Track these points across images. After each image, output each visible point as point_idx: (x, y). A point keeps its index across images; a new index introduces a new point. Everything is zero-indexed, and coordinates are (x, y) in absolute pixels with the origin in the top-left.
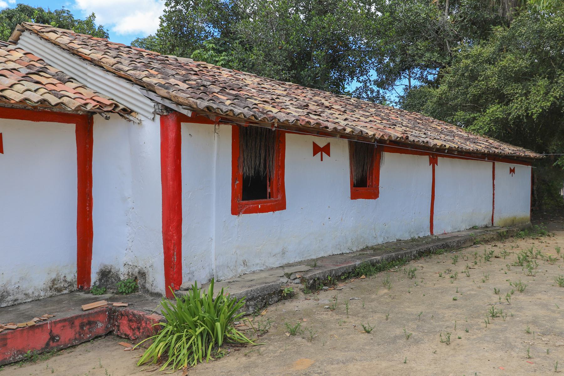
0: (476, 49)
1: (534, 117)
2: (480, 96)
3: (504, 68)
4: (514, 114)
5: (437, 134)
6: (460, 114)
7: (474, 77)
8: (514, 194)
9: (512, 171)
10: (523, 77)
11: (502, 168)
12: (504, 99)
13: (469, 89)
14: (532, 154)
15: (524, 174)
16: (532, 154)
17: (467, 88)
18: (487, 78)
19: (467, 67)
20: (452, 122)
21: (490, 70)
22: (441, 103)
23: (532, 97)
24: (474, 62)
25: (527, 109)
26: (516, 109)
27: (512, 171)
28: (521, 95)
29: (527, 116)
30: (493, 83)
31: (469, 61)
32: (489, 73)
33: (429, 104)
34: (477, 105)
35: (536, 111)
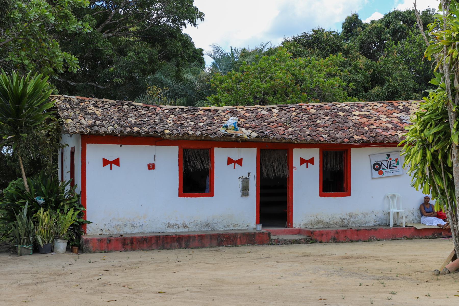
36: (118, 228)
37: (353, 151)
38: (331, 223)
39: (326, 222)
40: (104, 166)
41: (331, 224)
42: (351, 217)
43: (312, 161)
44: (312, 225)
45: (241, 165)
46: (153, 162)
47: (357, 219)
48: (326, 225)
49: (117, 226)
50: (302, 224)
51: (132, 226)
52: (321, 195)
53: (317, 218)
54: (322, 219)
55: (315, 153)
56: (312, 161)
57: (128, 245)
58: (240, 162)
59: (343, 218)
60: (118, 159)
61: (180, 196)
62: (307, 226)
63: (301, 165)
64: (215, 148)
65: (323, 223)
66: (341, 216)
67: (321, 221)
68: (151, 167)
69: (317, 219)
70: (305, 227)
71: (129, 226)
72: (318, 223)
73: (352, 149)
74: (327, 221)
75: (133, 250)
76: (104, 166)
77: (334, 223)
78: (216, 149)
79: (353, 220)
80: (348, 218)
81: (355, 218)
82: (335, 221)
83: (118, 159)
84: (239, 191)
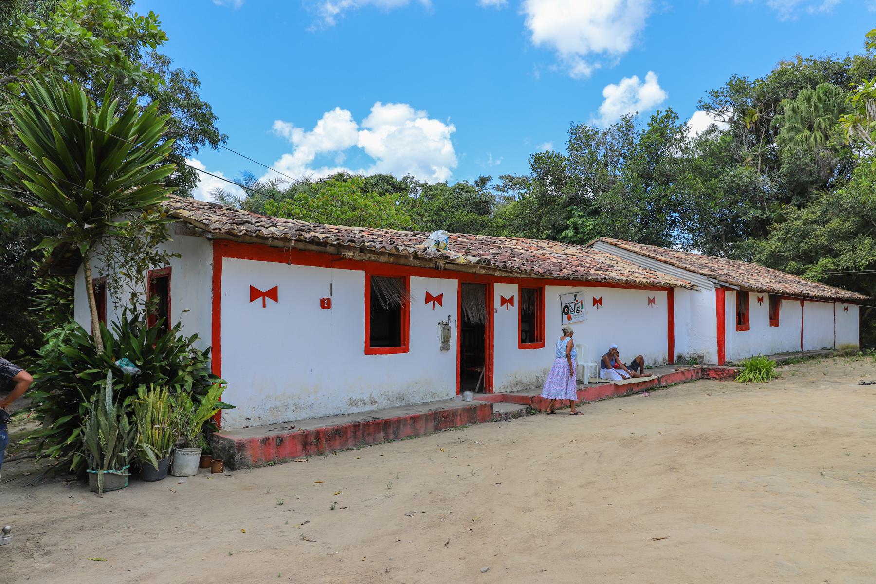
0: (805, 213)
1: (862, 268)
2: (811, 251)
3: (832, 230)
4: (844, 265)
5: (788, 283)
6: (793, 264)
7: (805, 235)
8: (846, 326)
9: (846, 309)
10: (849, 236)
11: (840, 307)
12: (836, 255)
13: (801, 245)
14: (862, 297)
15: (855, 310)
16: (862, 297)
17: (799, 244)
18: (817, 237)
19: (798, 228)
20: (784, 270)
21: (820, 230)
22: (772, 255)
23: (858, 253)
24: (804, 224)
25: (855, 262)
26: (845, 261)
27: (846, 309)
28: (849, 251)
29: (855, 267)
30: (823, 240)
31: (799, 223)
32: (818, 232)
33: (763, 256)
34: (809, 258)
35: (863, 263)
36: (275, 413)
40: (252, 299)
45: (441, 304)
46: (328, 296)
49: (272, 409)
51: (297, 407)
57: (311, 444)
58: (439, 299)
60: (275, 289)
61: (367, 352)
64: (412, 277)
68: (326, 304)
71: (292, 408)
75: (321, 454)
76: (252, 299)
78: (412, 277)
83: (275, 289)
84: (439, 345)
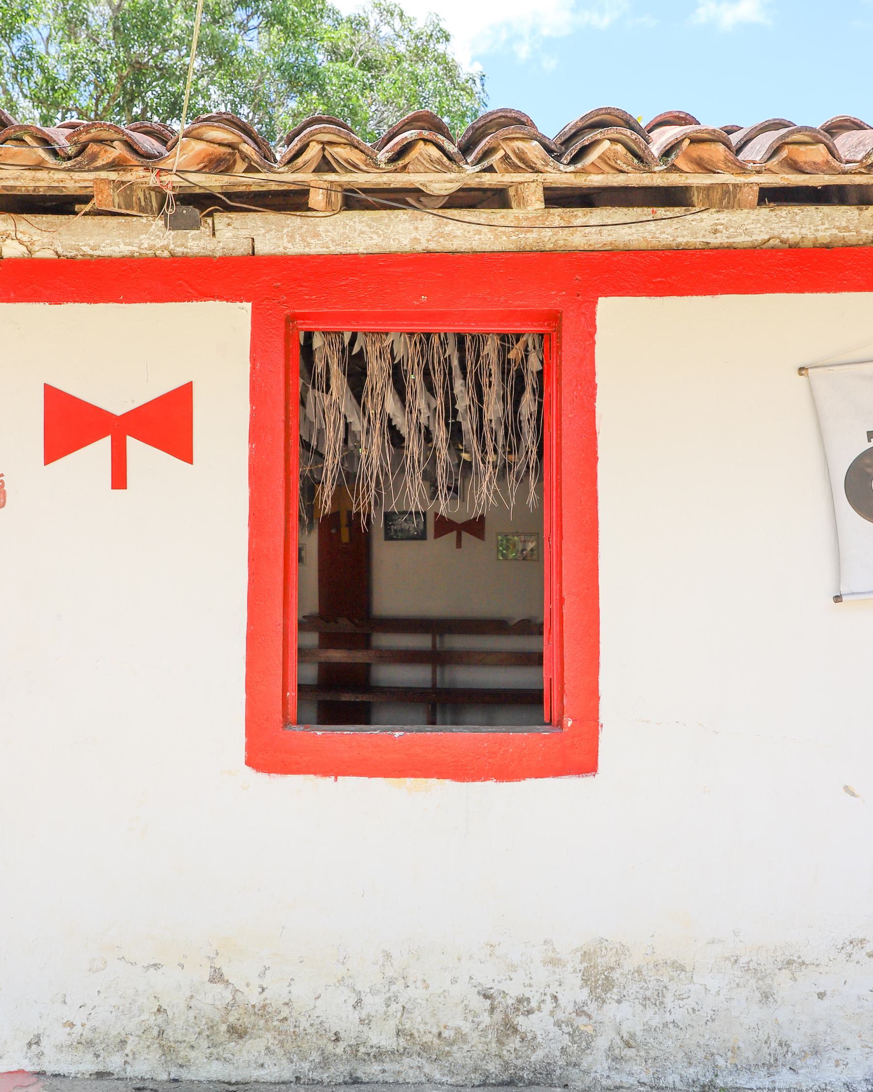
37: (614, 314)
38: (382, 1037)
39: (321, 1029)
41: (379, 1055)
42: (600, 982)
43: (168, 423)
44: (167, 1051)
47: (679, 1015)
48: (326, 1061)
50: (60, 1035)
52: (266, 754)
53: (217, 977)
54: (276, 994)
55: (210, 347)
56: (168, 423)
59: (515, 990)
62: (114, 1063)
63: (52, 453)
65: (291, 1039)
66: (488, 977)
67: (263, 1011)
69: (219, 994)
70: (89, 1065)
72: (237, 1033)
73: (607, 308)
74: (339, 1014)
77: (410, 1044)
79: (622, 1015)
80: (574, 993)
81: (655, 1000)
82: (415, 1023)
